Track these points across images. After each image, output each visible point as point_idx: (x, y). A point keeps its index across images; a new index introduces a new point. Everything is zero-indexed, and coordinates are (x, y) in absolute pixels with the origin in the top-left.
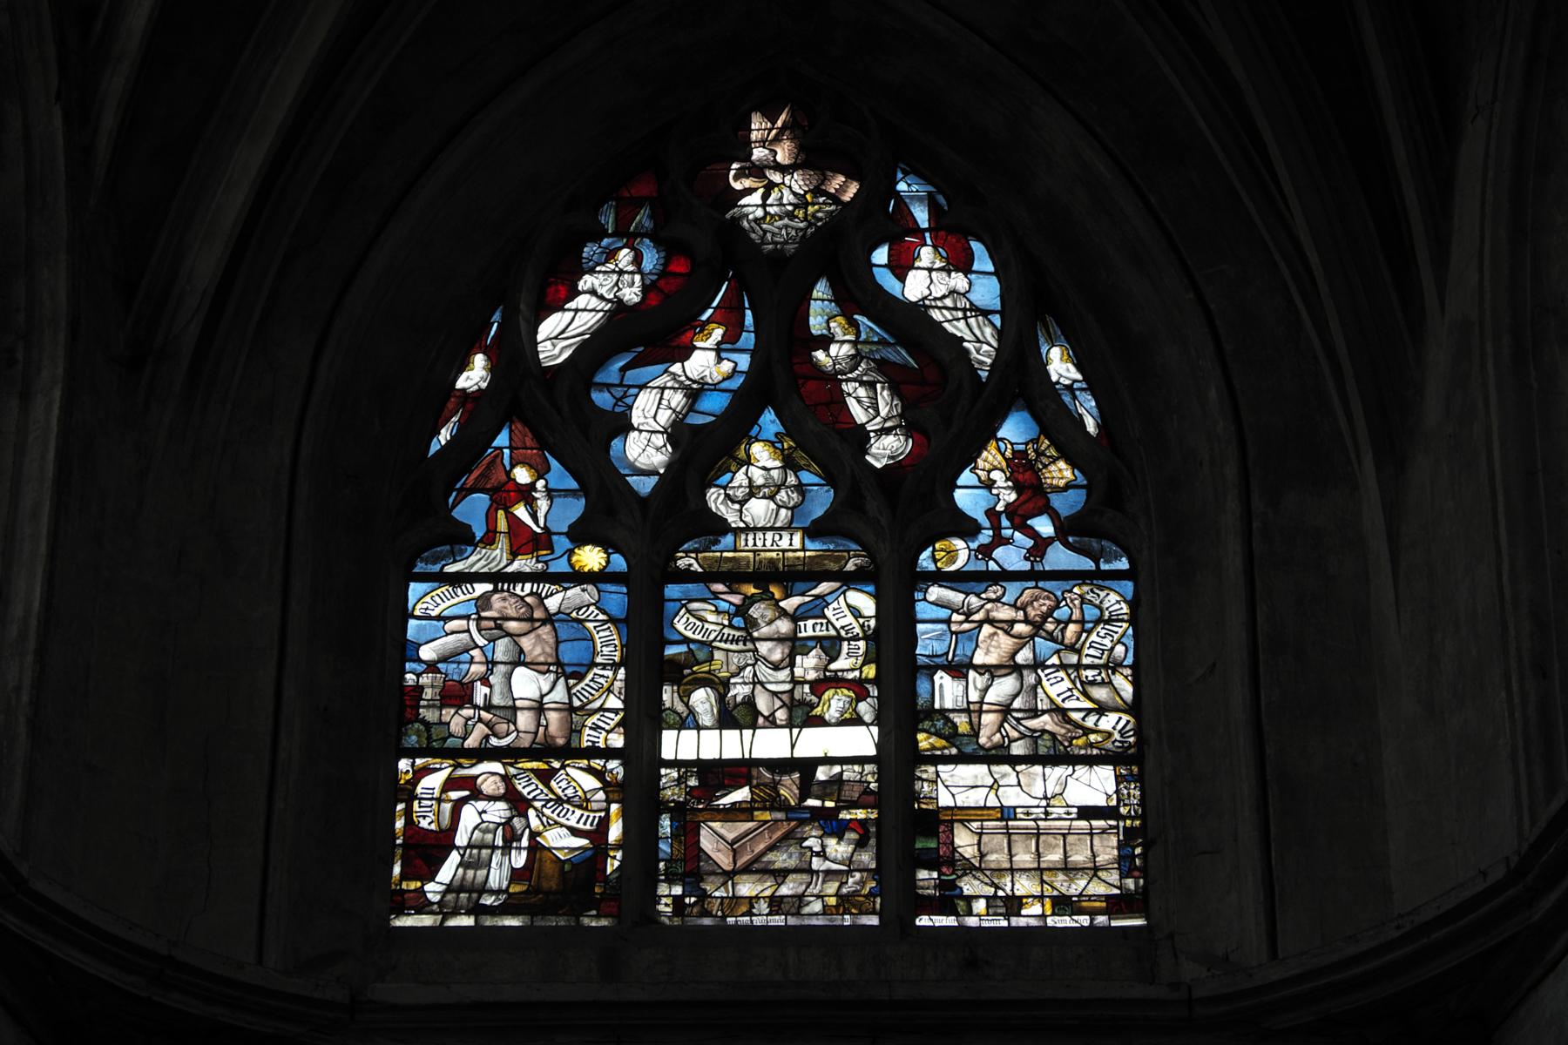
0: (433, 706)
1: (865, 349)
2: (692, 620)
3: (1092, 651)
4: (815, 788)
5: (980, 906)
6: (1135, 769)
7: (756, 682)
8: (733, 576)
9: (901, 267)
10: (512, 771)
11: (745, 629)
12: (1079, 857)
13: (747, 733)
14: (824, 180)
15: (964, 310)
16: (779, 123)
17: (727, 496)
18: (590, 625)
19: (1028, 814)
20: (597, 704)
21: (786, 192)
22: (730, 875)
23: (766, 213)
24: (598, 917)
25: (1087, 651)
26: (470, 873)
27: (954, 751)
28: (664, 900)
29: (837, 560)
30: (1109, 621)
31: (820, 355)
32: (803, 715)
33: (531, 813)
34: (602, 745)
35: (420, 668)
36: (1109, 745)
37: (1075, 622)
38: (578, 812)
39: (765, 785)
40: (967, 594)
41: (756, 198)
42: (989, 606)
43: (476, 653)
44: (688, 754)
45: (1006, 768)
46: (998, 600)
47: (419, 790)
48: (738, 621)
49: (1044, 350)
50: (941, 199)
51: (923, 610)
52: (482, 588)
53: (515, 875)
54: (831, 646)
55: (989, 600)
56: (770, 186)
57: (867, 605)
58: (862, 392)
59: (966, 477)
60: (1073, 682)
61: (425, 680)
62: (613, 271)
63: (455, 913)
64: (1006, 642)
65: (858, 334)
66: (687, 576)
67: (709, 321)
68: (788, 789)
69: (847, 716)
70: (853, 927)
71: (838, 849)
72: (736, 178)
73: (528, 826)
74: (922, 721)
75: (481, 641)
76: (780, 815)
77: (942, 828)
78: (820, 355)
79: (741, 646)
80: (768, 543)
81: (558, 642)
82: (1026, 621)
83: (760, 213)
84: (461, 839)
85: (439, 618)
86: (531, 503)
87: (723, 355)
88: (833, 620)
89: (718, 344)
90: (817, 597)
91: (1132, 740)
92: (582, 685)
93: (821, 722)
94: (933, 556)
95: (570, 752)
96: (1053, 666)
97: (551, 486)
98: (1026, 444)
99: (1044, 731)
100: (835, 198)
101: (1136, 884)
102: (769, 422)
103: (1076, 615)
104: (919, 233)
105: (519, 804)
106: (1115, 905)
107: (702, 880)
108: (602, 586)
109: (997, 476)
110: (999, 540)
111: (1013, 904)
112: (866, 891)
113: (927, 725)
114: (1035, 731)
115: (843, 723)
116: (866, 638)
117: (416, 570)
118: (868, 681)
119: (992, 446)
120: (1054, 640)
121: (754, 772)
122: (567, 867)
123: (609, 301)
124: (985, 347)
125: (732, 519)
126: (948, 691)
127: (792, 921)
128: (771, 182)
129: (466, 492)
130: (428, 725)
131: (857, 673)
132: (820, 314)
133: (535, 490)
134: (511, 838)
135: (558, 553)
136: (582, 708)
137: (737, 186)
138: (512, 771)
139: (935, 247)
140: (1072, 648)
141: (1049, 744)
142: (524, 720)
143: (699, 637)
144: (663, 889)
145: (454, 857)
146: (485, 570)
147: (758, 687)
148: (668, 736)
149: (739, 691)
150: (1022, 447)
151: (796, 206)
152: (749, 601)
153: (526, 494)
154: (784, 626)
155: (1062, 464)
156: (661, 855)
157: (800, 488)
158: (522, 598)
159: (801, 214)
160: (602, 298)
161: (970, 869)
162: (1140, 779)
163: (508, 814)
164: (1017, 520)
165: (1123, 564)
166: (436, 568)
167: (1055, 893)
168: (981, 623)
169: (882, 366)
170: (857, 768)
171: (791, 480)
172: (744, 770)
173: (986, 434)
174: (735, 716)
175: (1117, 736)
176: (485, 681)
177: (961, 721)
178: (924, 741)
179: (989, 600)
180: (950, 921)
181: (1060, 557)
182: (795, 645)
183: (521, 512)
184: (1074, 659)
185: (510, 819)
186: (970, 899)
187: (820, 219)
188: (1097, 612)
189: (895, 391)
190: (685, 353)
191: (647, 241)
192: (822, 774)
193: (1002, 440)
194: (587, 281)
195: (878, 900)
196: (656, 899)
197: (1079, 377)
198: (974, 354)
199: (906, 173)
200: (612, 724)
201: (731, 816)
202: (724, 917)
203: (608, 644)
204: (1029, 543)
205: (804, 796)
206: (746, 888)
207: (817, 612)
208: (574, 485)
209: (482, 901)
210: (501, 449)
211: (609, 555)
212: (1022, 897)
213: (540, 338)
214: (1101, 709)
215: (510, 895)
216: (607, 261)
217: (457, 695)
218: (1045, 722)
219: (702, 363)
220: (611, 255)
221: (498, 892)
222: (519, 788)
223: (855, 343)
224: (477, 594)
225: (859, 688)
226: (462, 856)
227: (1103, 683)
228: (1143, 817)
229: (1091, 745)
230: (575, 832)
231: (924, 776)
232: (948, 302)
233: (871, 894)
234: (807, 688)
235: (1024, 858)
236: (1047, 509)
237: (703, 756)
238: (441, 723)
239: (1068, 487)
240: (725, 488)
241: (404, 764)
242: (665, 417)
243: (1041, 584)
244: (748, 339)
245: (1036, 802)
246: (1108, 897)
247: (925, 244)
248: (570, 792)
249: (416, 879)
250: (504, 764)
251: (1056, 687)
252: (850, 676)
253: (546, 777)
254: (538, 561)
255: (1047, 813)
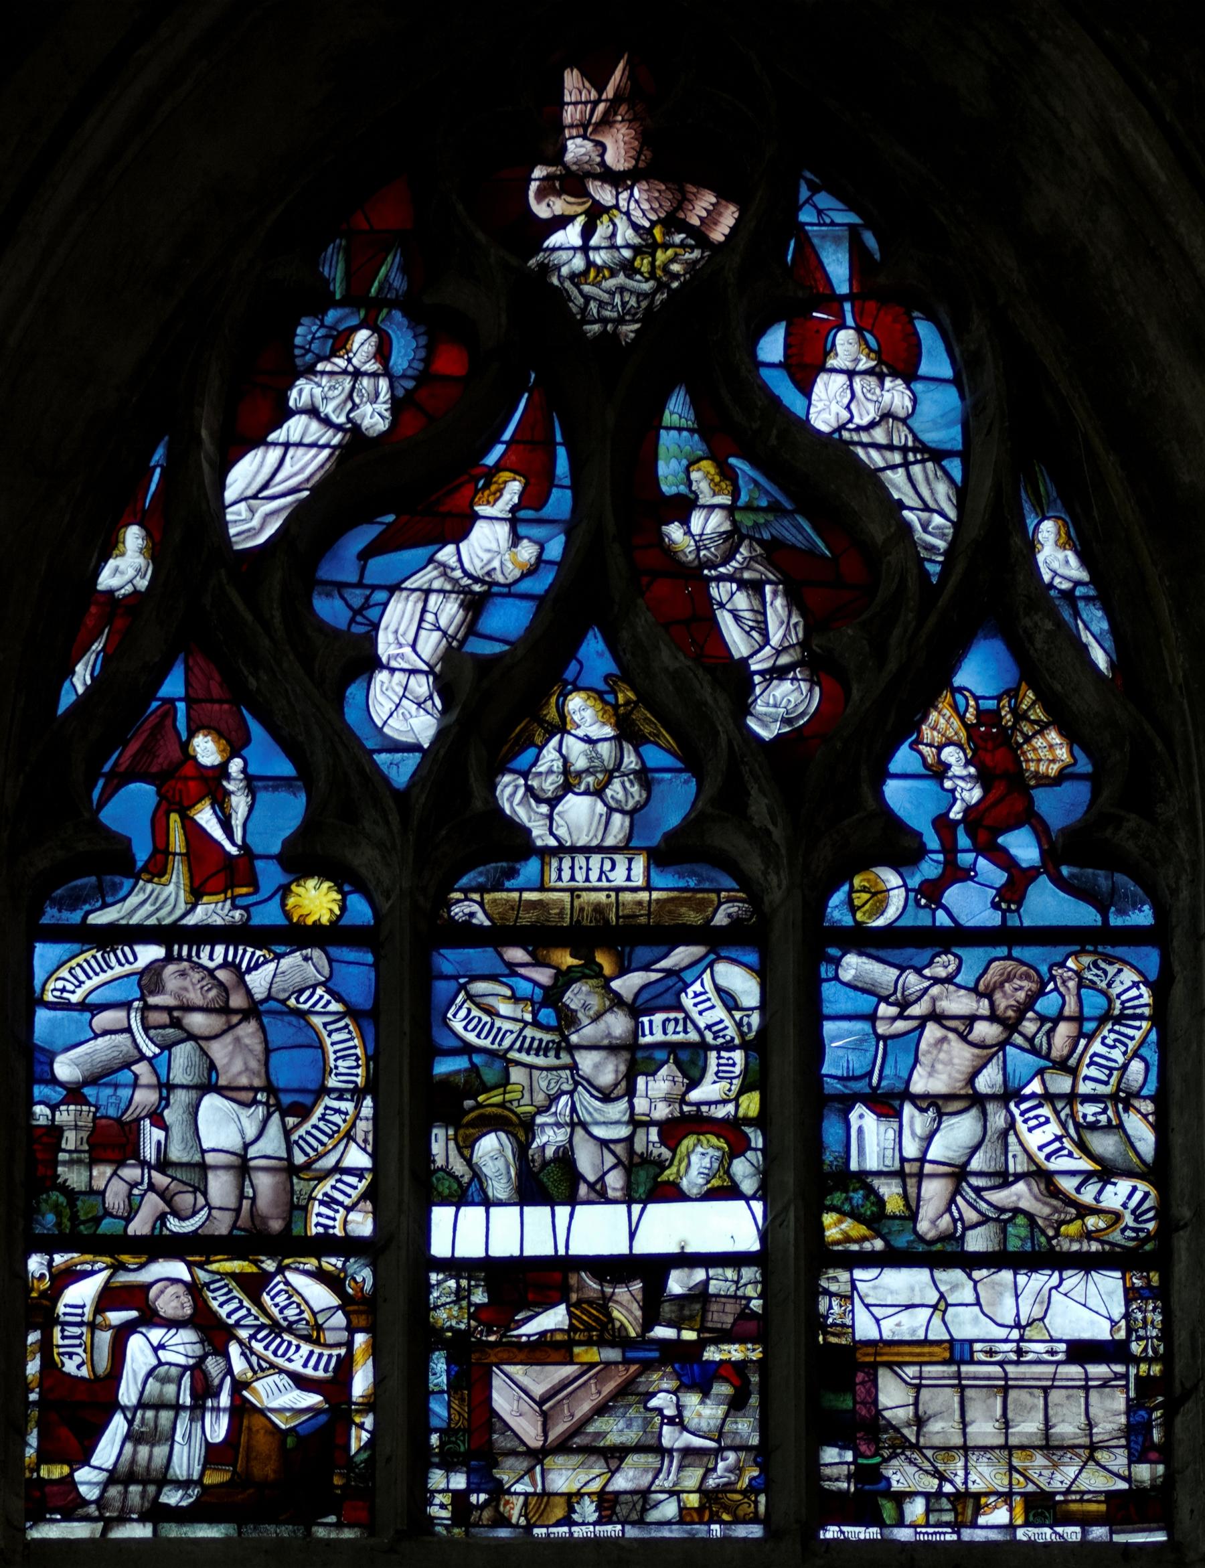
0: (79, 1162)
1: (746, 520)
2: (475, 1012)
3: (1093, 1072)
4: (667, 1310)
5: (916, 1509)
6: (1155, 1278)
7: (576, 1123)
8: (540, 936)
9: (806, 367)
10: (203, 1276)
11: (558, 1029)
12: (1068, 1427)
13: (563, 1211)
14: (682, 201)
15: (904, 450)
16: (609, 92)
17: (529, 789)
18: (317, 1021)
19: (991, 1353)
20: (329, 1162)
21: (621, 223)
22: (538, 1456)
23: (590, 264)
24: (339, 1525)
25: (1085, 1071)
26: (144, 1451)
27: (879, 1244)
28: (439, 1498)
29: (700, 906)
30: (1120, 1019)
31: (675, 532)
32: (650, 1184)
33: (234, 1349)
34: (338, 1232)
35: (57, 1094)
36: (1116, 1236)
37: (1069, 1019)
38: (306, 1348)
39: (590, 1302)
40: (902, 969)
41: (571, 235)
42: (935, 990)
43: (141, 1068)
44: (469, 1247)
45: (957, 1275)
46: (949, 980)
47: (61, 1309)
48: (547, 1015)
49: (1031, 522)
50: (870, 240)
51: (834, 998)
52: (149, 953)
53: (213, 1455)
54: (690, 1060)
55: (937, 981)
56: (596, 212)
57: (744, 985)
58: (742, 601)
59: (904, 759)
60: (1064, 1125)
61: (65, 1116)
62: (345, 372)
63: (123, 1519)
64: (961, 1055)
65: (735, 494)
66: (467, 935)
67: (499, 467)
68: (626, 1306)
69: (716, 1182)
70: (726, 1540)
71: (704, 1412)
72: (541, 195)
73: (229, 1371)
74: (830, 1192)
75: (149, 1049)
76: (613, 1354)
77: (860, 1377)
78: (675, 532)
79: (551, 1061)
80: (594, 875)
81: (268, 1051)
82: (993, 1018)
83: (578, 263)
84: (128, 1394)
85: (83, 1006)
86: (221, 802)
87: (522, 530)
88: (694, 1014)
89: (514, 509)
90: (669, 973)
91: (1151, 1226)
92: (307, 1126)
93: (673, 1193)
94: (850, 901)
95: (292, 1244)
96: (1033, 1095)
97: (252, 770)
98: (999, 698)
99: (1017, 1211)
100: (699, 236)
101: (1153, 1472)
102: (595, 655)
103: (1071, 1009)
104: (832, 301)
105: (214, 1334)
106: (1123, 1507)
107: (496, 1465)
108: (334, 951)
109: (951, 755)
110: (955, 873)
111: (967, 1504)
112: (744, 1483)
113: (837, 1198)
114: (1002, 1210)
115: (711, 1195)
116: (745, 1046)
117: (45, 920)
118: (748, 1121)
119: (946, 696)
120: (1034, 1051)
121: (573, 1280)
122: (290, 1441)
123: (339, 428)
124: (937, 520)
125: (541, 836)
126: (872, 1140)
127: (632, 1532)
128: (596, 203)
129: (118, 780)
130: (71, 1195)
131: (730, 1108)
132: (676, 459)
133: (228, 777)
134: (204, 1391)
135: (265, 893)
136: (307, 1166)
137: (542, 211)
138: (203, 1276)
139: (859, 330)
140: (1063, 1066)
141: (1024, 1232)
142: (220, 1187)
143: (486, 1043)
144: (437, 1479)
145: (118, 1425)
146: (152, 921)
147: (579, 1132)
148: (441, 1216)
149: (550, 1138)
150: (991, 704)
151: (637, 250)
152: (565, 979)
153: (212, 785)
154: (618, 1024)
155: (1053, 736)
156: (435, 1422)
157: (644, 776)
158: (211, 972)
159: (644, 264)
160: (326, 422)
161: (901, 1447)
162: (1162, 1294)
163: (198, 1350)
164: (983, 836)
165: (1143, 917)
166: (75, 917)
167: (1031, 1488)
168: (923, 1020)
169: (775, 553)
170: (730, 1273)
171: (630, 761)
172: (557, 1276)
173: (935, 681)
174: (547, 1183)
175: (1129, 1220)
176: (158, 1120)
177: (889, 1191)
178: (834, 1227)
179: (937, 981)
180: (873, 1533)
181: (1047, 904)
182: (637, 1059)
183: (206, 818)
184: (1062, 1084)
185: (202, 1359)
186: (901, 1498)
187: (676, 276)
188: (1102, 1001)
189: (794, 600)
190: (460, 533)
191: (397, 315)
192: (677, 1283)
193: (961, 690)
194: (302, 392)
195: (762, 1499)
196: (425, 1496)
197: (1084, 576)
198: (919, 533)
199: (814, 189)
200: (354, 1194)
201: (538, 1355)
202: (529, 1527)
203: (345, 1054)
204: (999, 877)
205: (649, 1322)
206: (564, 1477)
207: (668, 999)
208: (286, 768)
209: (163, 1499)
210: (170, 702)
211: (344, 895)
212: (977, 1496)
213: (230, 495)
214: (1106, 1173)
215: (206, 1489)
216: (334, 353)
217: (115, 1141)
218: (1020, 1194)
219: (487, 546)
220: (340, 342)
221: (185, 1484)
222: (214, 1305)
223: (730, 510)
224: (141, 964)
225: (732, 1133)
226: (130, 1422)
227: (1109, 1126)
228: (1166, 1359)
229: (1089, 1235)
230: (301, 1382)
231: (833, 1288)
232: (879, 435)
233: (752, 1490)
234: (654, 1131)
235: (984, 1429)
236: (1029, 818)
237: (495, 1252)
238: (91, 1192)
239: (1063, 776)
240: (525, 775)
241: (36, 1264)
242: (430, 643)
243: (1016, 952)
244: (560, 502)
245: (1002, 1333)
246: (1111, 1495)
247: (843, 326)
248: (291, 1312)
249: (61, 1461)
250: (190, 1265)
251: (1038, 1135)
252: (721, 1112)
253: (254, 1286)
254: (235, 907)
255: (1020, 1352)
